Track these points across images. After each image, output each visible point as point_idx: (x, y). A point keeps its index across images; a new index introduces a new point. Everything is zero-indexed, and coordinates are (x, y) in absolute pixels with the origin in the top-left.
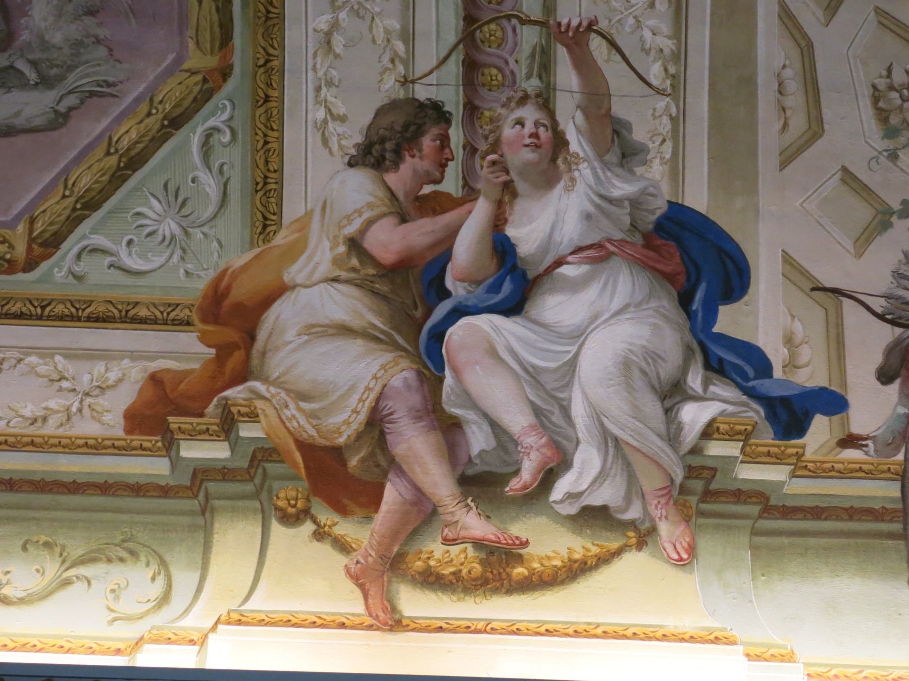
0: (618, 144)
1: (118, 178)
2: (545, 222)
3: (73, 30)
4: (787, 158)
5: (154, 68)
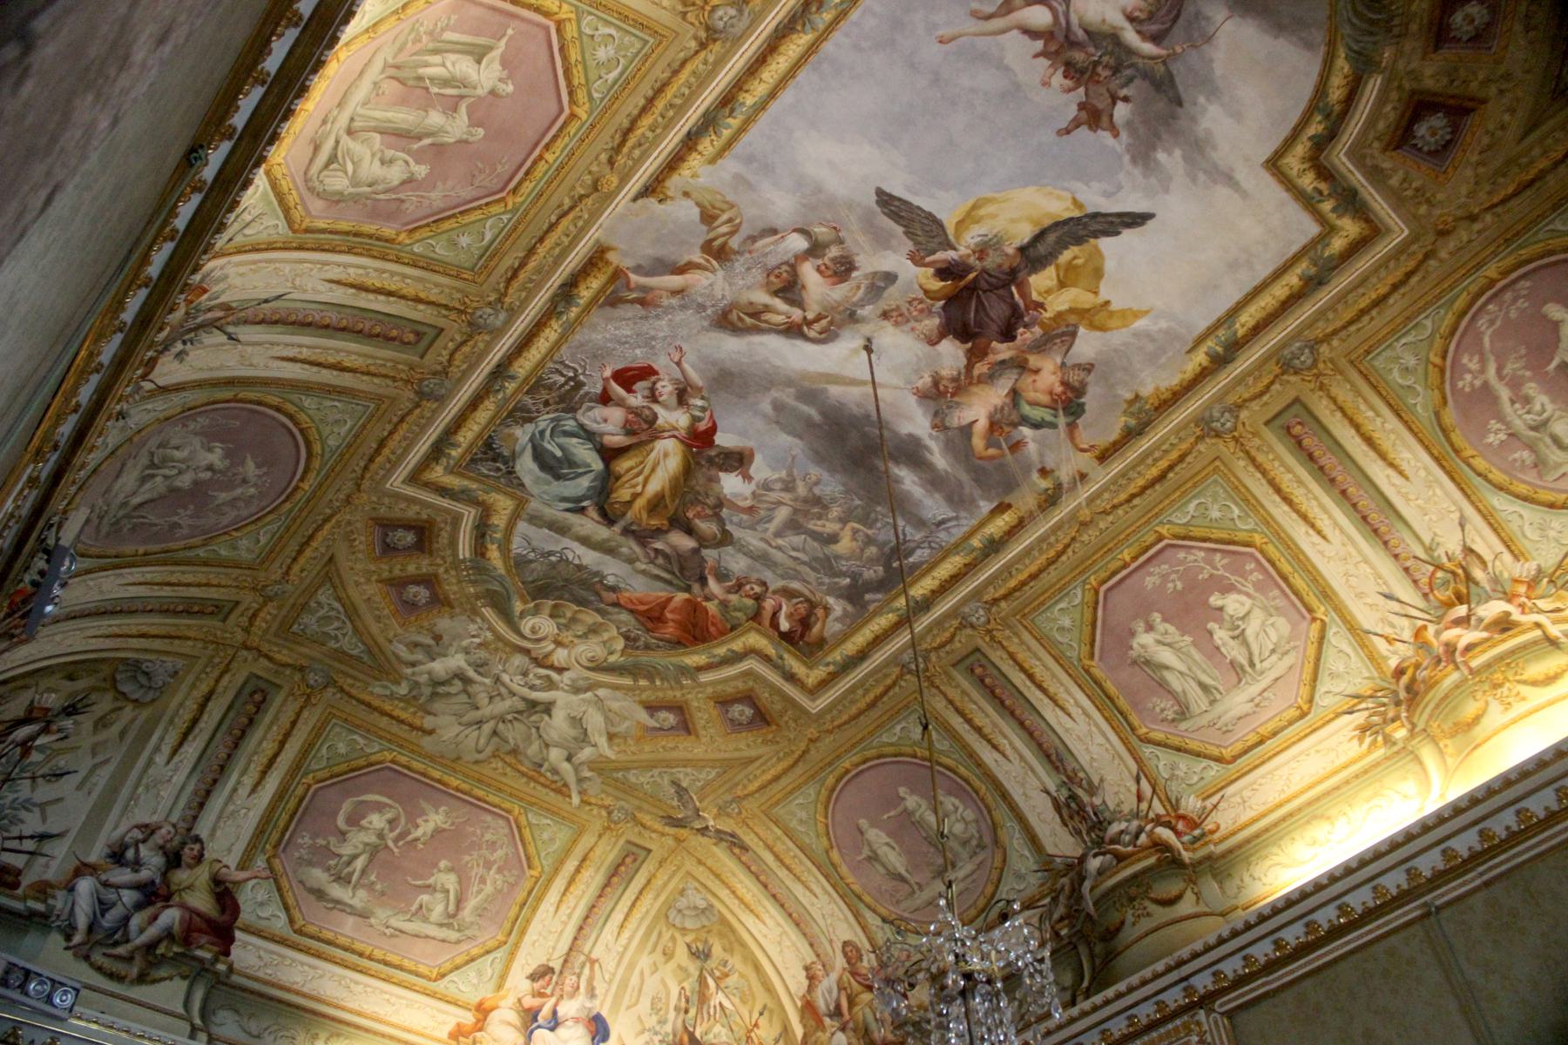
0: (592, 994)
1: (467, 963)
4: (628, 1008)
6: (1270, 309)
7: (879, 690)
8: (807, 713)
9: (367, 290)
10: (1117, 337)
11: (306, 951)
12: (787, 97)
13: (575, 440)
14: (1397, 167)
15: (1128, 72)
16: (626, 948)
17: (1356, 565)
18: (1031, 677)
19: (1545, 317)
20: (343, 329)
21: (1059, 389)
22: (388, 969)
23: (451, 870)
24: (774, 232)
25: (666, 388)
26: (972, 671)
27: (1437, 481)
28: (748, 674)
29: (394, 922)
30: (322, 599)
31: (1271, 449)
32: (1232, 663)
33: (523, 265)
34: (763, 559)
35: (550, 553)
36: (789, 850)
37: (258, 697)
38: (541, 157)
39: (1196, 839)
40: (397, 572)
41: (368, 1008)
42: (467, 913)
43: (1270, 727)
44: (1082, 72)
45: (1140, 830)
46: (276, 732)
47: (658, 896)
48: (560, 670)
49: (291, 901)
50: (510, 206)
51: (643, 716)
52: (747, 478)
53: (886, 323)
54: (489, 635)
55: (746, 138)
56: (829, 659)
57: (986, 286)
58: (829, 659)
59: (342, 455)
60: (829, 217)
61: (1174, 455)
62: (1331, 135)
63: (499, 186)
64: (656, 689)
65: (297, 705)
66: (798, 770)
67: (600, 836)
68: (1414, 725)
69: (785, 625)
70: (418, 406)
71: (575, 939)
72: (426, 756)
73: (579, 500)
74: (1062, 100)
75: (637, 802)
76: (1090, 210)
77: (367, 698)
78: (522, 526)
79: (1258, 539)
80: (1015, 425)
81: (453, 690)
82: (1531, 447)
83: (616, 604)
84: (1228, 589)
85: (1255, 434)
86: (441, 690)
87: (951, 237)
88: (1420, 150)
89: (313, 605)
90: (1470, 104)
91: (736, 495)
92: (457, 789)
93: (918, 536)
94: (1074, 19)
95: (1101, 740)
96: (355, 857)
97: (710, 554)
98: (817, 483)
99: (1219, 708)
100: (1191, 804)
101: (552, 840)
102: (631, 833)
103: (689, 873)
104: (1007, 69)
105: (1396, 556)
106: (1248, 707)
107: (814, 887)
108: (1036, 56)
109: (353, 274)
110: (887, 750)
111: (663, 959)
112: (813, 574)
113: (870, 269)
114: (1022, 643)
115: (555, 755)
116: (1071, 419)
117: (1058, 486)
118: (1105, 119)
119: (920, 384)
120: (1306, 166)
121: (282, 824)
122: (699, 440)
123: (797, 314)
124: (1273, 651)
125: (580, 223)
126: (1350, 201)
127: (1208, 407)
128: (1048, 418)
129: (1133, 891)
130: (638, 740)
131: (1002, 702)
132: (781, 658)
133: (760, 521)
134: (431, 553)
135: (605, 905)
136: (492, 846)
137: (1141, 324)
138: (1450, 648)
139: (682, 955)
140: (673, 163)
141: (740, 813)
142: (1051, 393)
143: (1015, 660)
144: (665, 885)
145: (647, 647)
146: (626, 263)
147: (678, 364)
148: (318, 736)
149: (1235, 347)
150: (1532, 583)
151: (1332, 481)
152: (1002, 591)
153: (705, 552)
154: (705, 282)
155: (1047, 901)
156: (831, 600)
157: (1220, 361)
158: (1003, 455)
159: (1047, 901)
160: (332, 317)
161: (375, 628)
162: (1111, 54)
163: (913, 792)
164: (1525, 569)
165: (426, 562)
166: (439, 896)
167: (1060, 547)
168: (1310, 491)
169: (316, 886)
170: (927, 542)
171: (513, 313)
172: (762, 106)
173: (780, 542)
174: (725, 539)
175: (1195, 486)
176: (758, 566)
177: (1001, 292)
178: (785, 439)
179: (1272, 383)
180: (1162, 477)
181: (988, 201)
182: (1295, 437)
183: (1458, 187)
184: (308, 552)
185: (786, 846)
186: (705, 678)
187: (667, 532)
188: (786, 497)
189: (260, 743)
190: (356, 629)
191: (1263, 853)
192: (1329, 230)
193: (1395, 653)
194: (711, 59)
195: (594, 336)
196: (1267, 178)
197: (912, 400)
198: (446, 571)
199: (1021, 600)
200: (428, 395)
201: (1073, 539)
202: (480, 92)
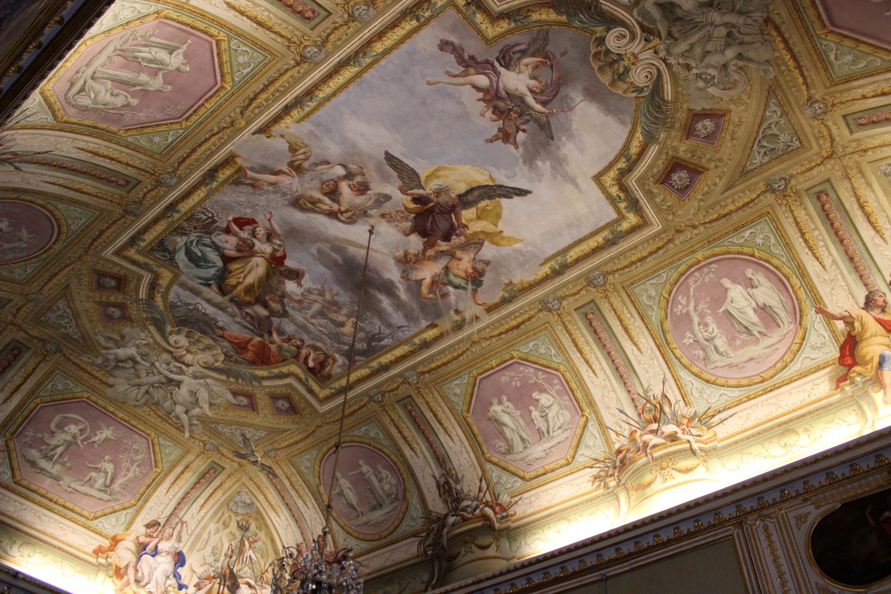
0: (179, 539)
1: (111, 513)
2: (164, 546)
3: (119, 489)
5: (126, 500)
6: (586, 252)
7: (357, 407)
8: (316, 411)
9: (99, 155)
10: (505, 250)
11: (20, 495)
12: (342, 96)
13: (209, 249)
14: (661, 193)
15: (527, 117)
16: (203, 518)
17: (609, 392)
18: (435, 416)
19: (721, 285)
20: (84, 173)
21: (470, 271)
22: (66, 511)
23: (112, 461)
24: (328, 163)
25: (261, 231)
26: (406, 407)
27: (656, 357)
28: (289, 386)
29: (73, 485)
30: (61, 306)
31: (576, 324)
32: (538, 429)
33: (189, 156)
34: (303, 327)
35: (189, 304)
36: (298, 481)
37: (16, 352)
38: (203, 105)
39: (503, 517)
40: (104, 299)
41: (49, 530)
42: (116, 486)
43: (551, 466)
44: (502, 113)
45: (477, 507)
46: (23, 373)
47: (224, 494)
48: (188, 365)
49: (15, 465)
50: (183, 126)
51: (230, 397)
52: (300, 285)
53: (382, 220)
54: (151, 341)
55: (317, 113)
56: (332, 386)
57: (437, 211)
58: (332, 386)
59: (78, 235)
60: (358, 161)
61: (526, 316)
62: (629, 170)
63: (178, 116)
64: (238, 384)
65: (37, 360)
66: (309, 441)
67: (198, 456)
68: (620, 481)
69: (311, 364)
70: (123, 217)
71: (175, 509)
72: (107, 398)
73: (208, 279)
74: (490, 125)
75: (221, 441)
76: (498, 183)
77: (78, 362)
78: (175, 288)
79: (562, 368)
80: (445, 285)
81: (127, 366)
82: (704, 350)
83: (222, 337)
84: (543, 391)
85: (569, 314)
86: (120, 364)
87: (423, 183)
88: (673, 187)
89: (54, 308)
90: (701, 170)
91: (292, 292)
92: (121, 419)
93: (387, 332)
94: (501, 85)
95: (466, 456)
96: (57, 446)
97: (275, 320)
98: (337, 295)
99: (528, 452)
100: (505, 499)
101: (170, 454)
102: (215, 457)
103: (244, 484)
104: (462, 103)
105: (629, 392)
106: (543, 454)
107: (308, 503)
108: (479, 100)
109: (91, 147)
110: (356, 439)
111: (222, 527)
112: (329, 340)
113: (377, 191)
114: (434, 397)
115: (179, 409)
116: (474, 287)
117: (464, 320)
118: (512, 140)
119: (397, 254)
120: (615, 182)
121: (18, 422)
122: (276, 261)
123: (335, 207)
124: (560, 428)
125: (222, 141)
126: (635, 205)
127: (547, 295)
128: (463, 284)
129: (467, 538)
130: (226, 409)
131: (419, 426)
132: (307, 380)
133: (304, 308)
134: (124, 293)
135: (195, 493)
136: (137, 452)
137: (518, 246)
138: (645, 445)
139: (233, 526)
140: (277, 119)
141: (275, 457)
142: (466, 272)
143: (429, 406)
144: (230, 488)
145: (236, 362)
146: (245, 165)
147: (269, 220)
148: (47, 378)
149: (565, 268)
150: (691, 419)
151: (604, 346)
152: (427, 369)
153: (273, 319)
154: (288, 182)
155: (424, 534)
156: (337, 356)
157: (557, 273)
158: (437, 299)
159: (424, 534)
160: (78, 166)
161: (88, 326)
162: (519, 106)
163: (367, 463)
164: (689, 411)
165: (121, 297)
166: (102, 474)
167: (460, 352)
168: (592, 349)
169: (31, 459)
170: (391, 336)
171: (181, 180)
172: (328, 99)
173: (313, 321)
174: (284, 314)
175: (534, 334)
176: (300, 331)
177: (446, 216)
178: (322, 269)
179: (582, 289)
180: (518, 326)
181: (443, 168)
182: (589, 320)
183: (689, 210)
184: (55, 281)
185: (296, 478)
186: (265, 383)
187: (254, 305)
188: (320, 299)
189: (13, 377)
190: (77, 325)
191: (534, 531)
192: (622, 217)
193: (619, 441)
194: (302, 71)
195: (225, 198)
196: (593, 186)
197: (392, 262)
198: (131, 303)
199: (437, 375)
200: (131, 211)
201: (468, 349)
202: (170, 68)
